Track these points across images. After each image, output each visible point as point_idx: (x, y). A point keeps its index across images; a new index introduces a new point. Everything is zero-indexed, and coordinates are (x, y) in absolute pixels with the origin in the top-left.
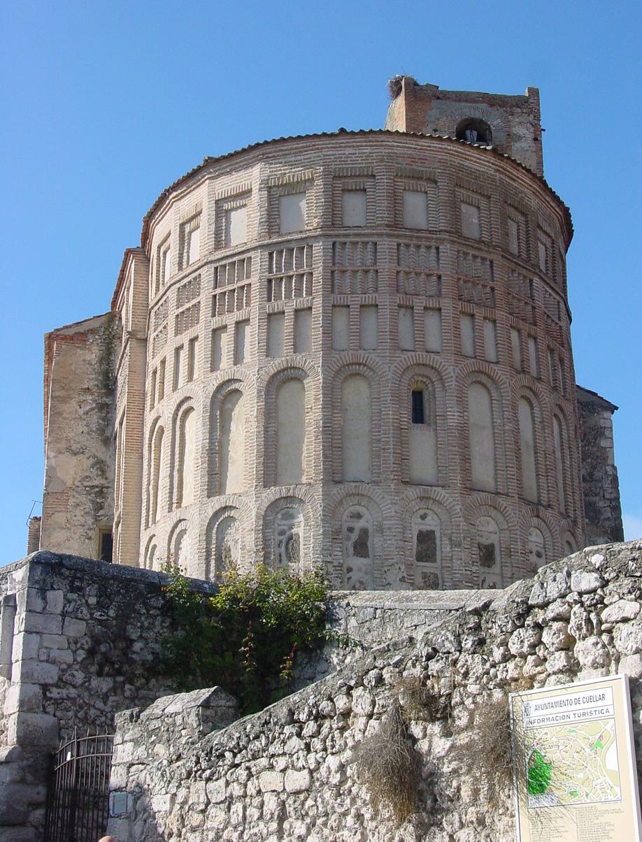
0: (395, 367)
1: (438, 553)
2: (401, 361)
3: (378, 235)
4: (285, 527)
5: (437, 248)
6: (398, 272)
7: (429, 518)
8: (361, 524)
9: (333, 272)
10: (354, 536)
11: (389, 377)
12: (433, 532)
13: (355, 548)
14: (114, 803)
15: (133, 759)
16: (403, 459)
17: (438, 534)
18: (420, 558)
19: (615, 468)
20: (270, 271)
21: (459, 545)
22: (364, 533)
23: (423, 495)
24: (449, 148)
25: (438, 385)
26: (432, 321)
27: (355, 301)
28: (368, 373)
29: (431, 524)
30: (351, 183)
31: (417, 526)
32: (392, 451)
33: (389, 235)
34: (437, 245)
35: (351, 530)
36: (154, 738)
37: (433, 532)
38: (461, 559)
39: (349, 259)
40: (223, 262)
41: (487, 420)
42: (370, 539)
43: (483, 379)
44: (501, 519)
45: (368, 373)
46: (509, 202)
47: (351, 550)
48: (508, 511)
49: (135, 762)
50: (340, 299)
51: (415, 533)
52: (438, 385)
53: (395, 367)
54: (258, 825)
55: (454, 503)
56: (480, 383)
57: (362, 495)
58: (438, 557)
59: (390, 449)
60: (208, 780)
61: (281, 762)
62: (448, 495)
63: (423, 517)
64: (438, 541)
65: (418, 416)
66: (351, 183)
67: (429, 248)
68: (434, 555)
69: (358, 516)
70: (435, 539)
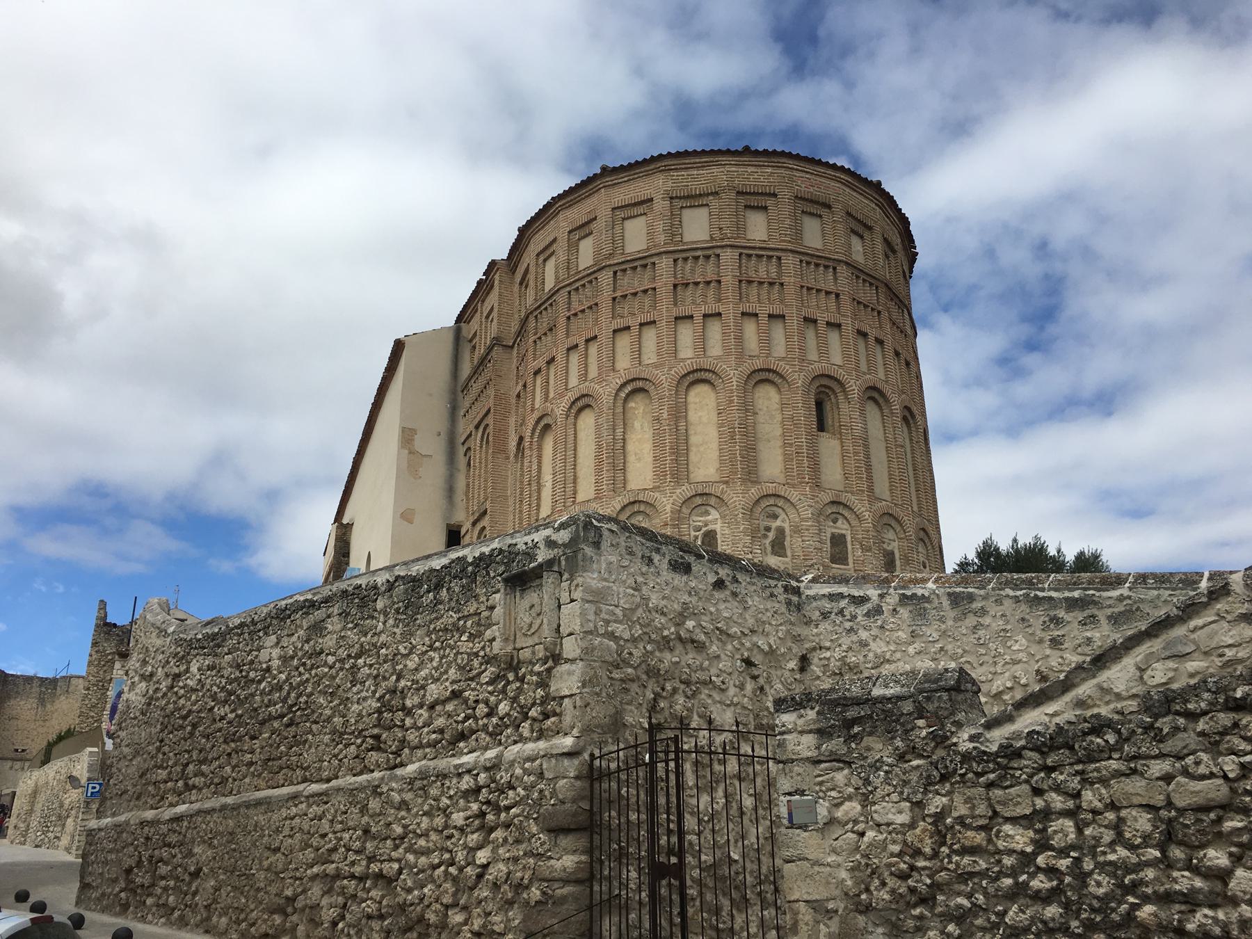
1: (850, 556)
3: (782, 250)
5: (835, 269)
7: (840, 522)
8: (778, 523)
10: (771, 535)
12: (844, 536)
13: (773, 547)
14: (790, 814)
15: (820, 754)
16: (815, 467)
17: (849, 538)
18: (834, 560)
20: (675, 277)
21: (869, 550)
22: (781, 531)
25: (841, 397)
26: (834, 337)
27: (764, 310)
28: (778, 380)
29: (842, 527)
30: (754, 201)
31: (830, 530)
35: (768, 529)
36: (856, 729)
37: (844, 536)
40: (624, 267)
41: (881, 435)
42: (788, 539)
43: (876, 395)
44: (898, 529)
45: (778, 380)
47: (769, 549)
49: (822, 758)
50: (748, 308)
51: (829, 536)
52: (841, 397)
54: (1115, 851)
57: (779, 496)
58: (850, 560)
60: (990, 785)
61: (1158, 768)
63: (835, 521)
64: (849, 547)
65: (821, 427)
66: (754, 201)
67: (826, 267)
68: (847, 559)
69: (775, 517)
70: (845, 542)
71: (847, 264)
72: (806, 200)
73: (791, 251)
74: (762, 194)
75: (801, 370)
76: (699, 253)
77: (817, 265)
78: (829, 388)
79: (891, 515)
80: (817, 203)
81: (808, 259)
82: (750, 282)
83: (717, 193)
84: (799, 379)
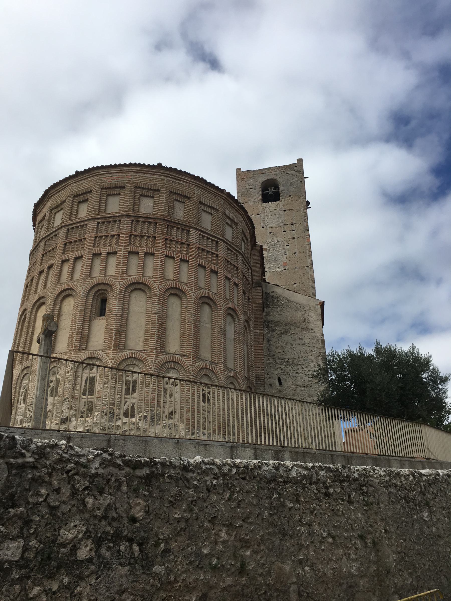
0: (86, 287)
2: (89, 283)
4: (25, 385)
6: (96, 237)
9: (65, 244)
11: (81, 293)
19: (323, 335)
23: (90, 356)
24: (132, 168)
30: (82, 198)
32: (76, 333)
33: (93, 219)
34: (120, 219)
38: (107, 392)
39: (74, 236)
46: (175, 191)
48: (147, 360)
53: (86, 287)
55: (108, 358)
56: (140, 289)
59: (75, 332)
62: (105, 354)
66: (82, 198)
71: (128, 216)
72: (110, 188)
73: (93, 219)
74: (85, 193)
75: (84, 285)
76: (53, 235)
77: (109, 222)
78: (102, 290)
79: (135, 358)
80: (116, 187)
81: (103, 220)
82: (71, 243)
83: (65, 201)
84: (81, 289)
